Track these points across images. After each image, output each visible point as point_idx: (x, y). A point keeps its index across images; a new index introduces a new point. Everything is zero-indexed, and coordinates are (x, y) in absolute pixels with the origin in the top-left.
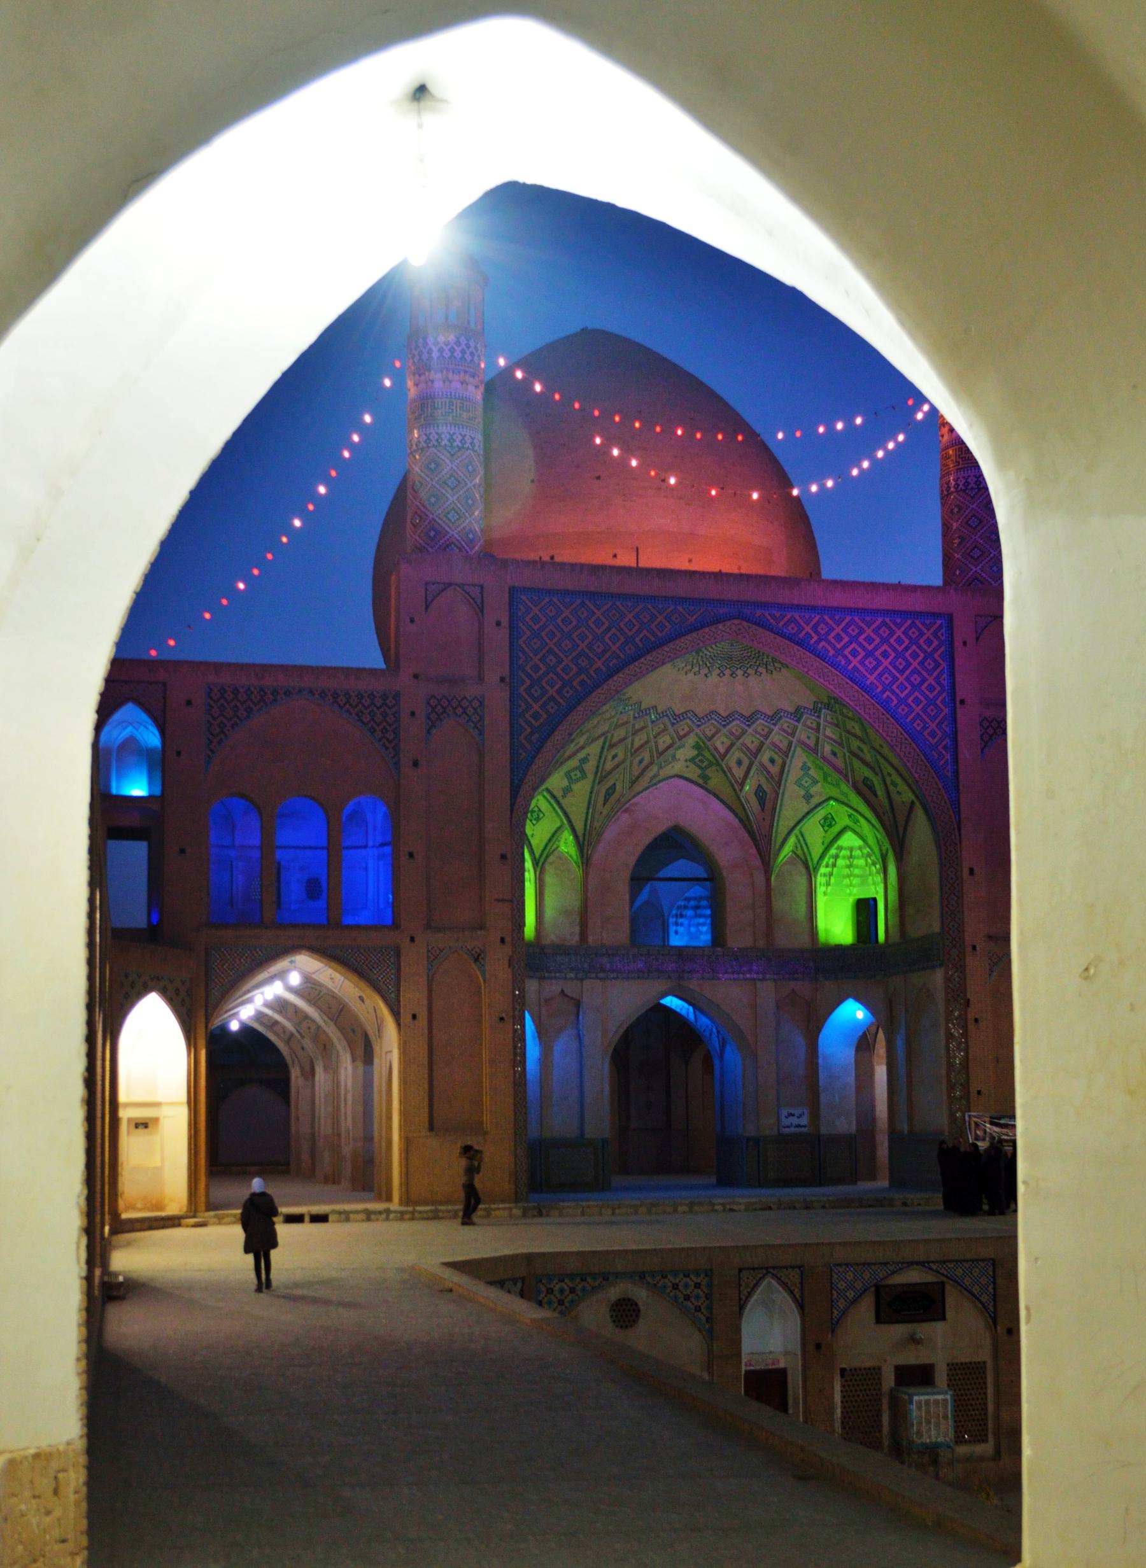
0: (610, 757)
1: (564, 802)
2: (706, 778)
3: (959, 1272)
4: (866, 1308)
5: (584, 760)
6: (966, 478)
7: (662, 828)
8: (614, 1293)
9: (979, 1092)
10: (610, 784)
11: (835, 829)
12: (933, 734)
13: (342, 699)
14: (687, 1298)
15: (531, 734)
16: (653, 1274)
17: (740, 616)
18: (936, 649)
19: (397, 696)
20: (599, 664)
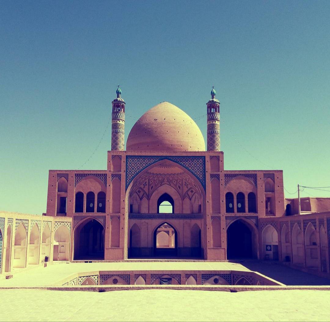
0: (150, 182)
1: (144, 189)
3: (174, 276)
5: (146, 182)
6: (210, 131)
7: (163, 193)
8: (113, 278)
9: (209, 242)
11: (193, 193)
12: (201, 178)
13: (97, 175)
14: (126, 279)
15: (129, 180)
16: (120, 275)
17: (166, 158)
19: (106, 174)
20: (141, 168)
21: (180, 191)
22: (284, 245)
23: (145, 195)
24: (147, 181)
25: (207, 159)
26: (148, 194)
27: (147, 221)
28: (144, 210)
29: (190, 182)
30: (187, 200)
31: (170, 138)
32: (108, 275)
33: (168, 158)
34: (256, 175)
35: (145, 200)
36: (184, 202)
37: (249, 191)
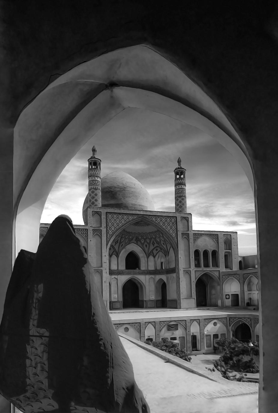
2: (137, 243)
3: (180, 322)
4: (164, 329)
7: (130, 251)
10: (122, 244)
15: (110, 236)
18: (174, 222)
21: (146, 249)
22: (246, 293)
23: (115, 252)
24: (119, 239)
25: (179, 219)
26: (117, 252)
27: (116, 276)
28: (114, 267)
29: (159, 240)
30: (151, 258)
31: (130, 201)
32: (120, 324)
33: (144, 216)
34: (217, 235)
35: (114, 257)
36: (149, 260)
37: (213, 249)
